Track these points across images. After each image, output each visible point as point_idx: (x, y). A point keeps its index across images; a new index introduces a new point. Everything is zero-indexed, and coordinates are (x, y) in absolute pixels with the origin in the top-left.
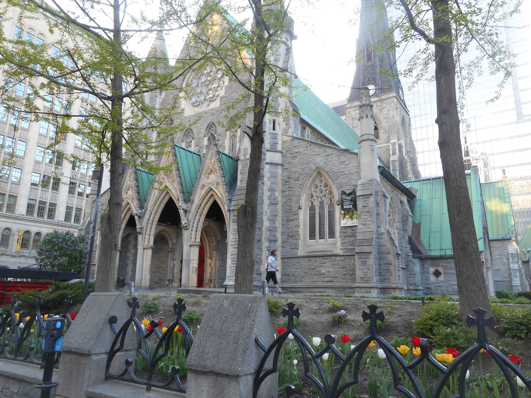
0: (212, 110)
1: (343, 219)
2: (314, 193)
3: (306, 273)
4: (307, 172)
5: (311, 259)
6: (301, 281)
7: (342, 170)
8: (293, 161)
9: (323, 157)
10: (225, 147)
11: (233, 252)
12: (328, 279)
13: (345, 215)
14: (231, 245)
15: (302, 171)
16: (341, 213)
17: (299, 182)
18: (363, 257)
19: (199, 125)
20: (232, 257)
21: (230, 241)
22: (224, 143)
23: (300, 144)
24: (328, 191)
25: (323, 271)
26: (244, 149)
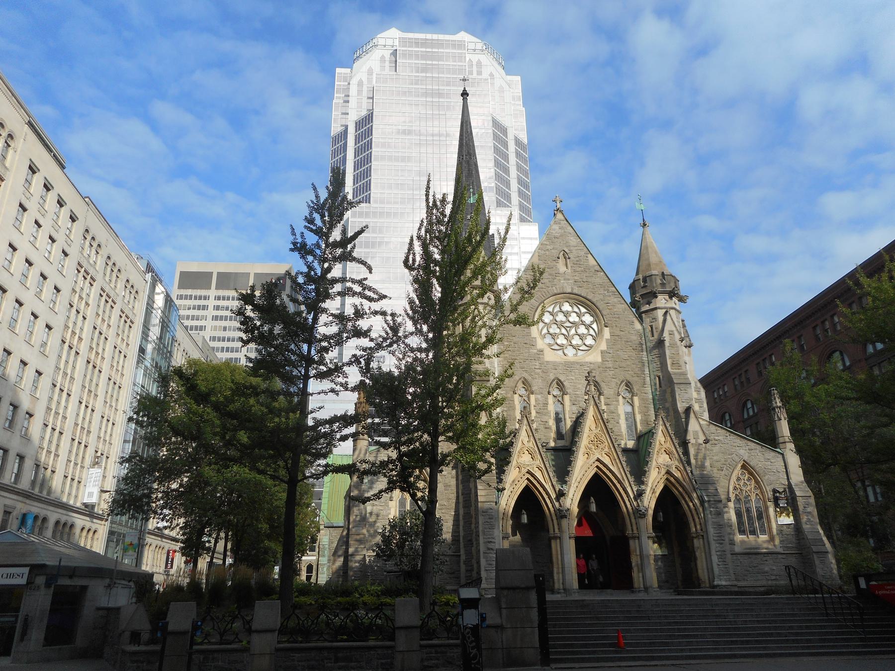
0: (591, 364)
1: (780, 516)
2: (737, 486)
3: (749, 571)
4: (731, 464)
5: (750, 556)
6: (744, 580)
7: (769, 467)
8: (713, 448)
9: (746, 450)
10: (619, 415)
11: (719, 549)
12: (774, 577)
13: (782, 513)
14: (714, 540)
15: (725, 461)
16: (776, 511)
17: (723, 473)
18: (821, 556)
19: (573, 378)
20: (718, 553)
21: (712, 537)
22: (617, 409)
23: (718, 432)
24: (753, 486)
25: (766, 569)
26: (693, 431)
